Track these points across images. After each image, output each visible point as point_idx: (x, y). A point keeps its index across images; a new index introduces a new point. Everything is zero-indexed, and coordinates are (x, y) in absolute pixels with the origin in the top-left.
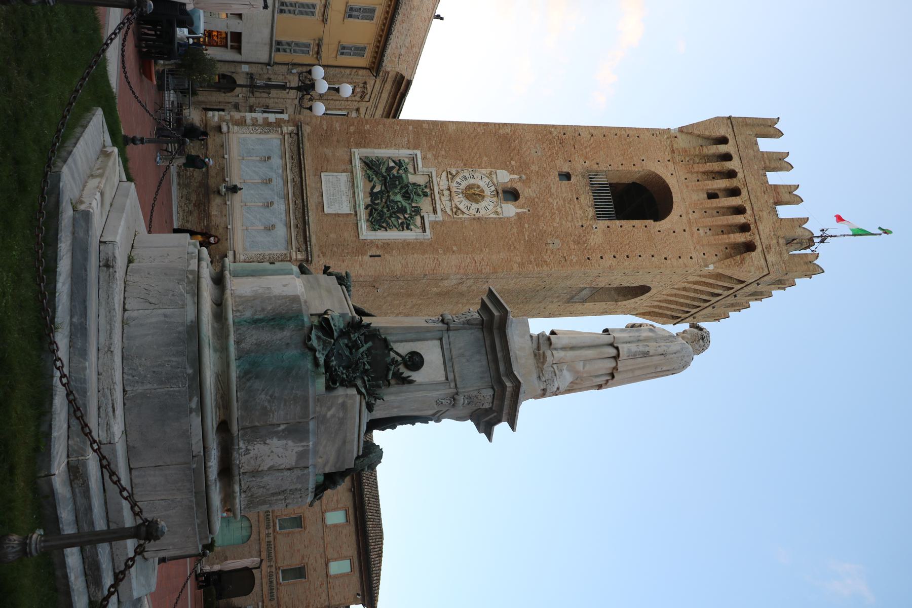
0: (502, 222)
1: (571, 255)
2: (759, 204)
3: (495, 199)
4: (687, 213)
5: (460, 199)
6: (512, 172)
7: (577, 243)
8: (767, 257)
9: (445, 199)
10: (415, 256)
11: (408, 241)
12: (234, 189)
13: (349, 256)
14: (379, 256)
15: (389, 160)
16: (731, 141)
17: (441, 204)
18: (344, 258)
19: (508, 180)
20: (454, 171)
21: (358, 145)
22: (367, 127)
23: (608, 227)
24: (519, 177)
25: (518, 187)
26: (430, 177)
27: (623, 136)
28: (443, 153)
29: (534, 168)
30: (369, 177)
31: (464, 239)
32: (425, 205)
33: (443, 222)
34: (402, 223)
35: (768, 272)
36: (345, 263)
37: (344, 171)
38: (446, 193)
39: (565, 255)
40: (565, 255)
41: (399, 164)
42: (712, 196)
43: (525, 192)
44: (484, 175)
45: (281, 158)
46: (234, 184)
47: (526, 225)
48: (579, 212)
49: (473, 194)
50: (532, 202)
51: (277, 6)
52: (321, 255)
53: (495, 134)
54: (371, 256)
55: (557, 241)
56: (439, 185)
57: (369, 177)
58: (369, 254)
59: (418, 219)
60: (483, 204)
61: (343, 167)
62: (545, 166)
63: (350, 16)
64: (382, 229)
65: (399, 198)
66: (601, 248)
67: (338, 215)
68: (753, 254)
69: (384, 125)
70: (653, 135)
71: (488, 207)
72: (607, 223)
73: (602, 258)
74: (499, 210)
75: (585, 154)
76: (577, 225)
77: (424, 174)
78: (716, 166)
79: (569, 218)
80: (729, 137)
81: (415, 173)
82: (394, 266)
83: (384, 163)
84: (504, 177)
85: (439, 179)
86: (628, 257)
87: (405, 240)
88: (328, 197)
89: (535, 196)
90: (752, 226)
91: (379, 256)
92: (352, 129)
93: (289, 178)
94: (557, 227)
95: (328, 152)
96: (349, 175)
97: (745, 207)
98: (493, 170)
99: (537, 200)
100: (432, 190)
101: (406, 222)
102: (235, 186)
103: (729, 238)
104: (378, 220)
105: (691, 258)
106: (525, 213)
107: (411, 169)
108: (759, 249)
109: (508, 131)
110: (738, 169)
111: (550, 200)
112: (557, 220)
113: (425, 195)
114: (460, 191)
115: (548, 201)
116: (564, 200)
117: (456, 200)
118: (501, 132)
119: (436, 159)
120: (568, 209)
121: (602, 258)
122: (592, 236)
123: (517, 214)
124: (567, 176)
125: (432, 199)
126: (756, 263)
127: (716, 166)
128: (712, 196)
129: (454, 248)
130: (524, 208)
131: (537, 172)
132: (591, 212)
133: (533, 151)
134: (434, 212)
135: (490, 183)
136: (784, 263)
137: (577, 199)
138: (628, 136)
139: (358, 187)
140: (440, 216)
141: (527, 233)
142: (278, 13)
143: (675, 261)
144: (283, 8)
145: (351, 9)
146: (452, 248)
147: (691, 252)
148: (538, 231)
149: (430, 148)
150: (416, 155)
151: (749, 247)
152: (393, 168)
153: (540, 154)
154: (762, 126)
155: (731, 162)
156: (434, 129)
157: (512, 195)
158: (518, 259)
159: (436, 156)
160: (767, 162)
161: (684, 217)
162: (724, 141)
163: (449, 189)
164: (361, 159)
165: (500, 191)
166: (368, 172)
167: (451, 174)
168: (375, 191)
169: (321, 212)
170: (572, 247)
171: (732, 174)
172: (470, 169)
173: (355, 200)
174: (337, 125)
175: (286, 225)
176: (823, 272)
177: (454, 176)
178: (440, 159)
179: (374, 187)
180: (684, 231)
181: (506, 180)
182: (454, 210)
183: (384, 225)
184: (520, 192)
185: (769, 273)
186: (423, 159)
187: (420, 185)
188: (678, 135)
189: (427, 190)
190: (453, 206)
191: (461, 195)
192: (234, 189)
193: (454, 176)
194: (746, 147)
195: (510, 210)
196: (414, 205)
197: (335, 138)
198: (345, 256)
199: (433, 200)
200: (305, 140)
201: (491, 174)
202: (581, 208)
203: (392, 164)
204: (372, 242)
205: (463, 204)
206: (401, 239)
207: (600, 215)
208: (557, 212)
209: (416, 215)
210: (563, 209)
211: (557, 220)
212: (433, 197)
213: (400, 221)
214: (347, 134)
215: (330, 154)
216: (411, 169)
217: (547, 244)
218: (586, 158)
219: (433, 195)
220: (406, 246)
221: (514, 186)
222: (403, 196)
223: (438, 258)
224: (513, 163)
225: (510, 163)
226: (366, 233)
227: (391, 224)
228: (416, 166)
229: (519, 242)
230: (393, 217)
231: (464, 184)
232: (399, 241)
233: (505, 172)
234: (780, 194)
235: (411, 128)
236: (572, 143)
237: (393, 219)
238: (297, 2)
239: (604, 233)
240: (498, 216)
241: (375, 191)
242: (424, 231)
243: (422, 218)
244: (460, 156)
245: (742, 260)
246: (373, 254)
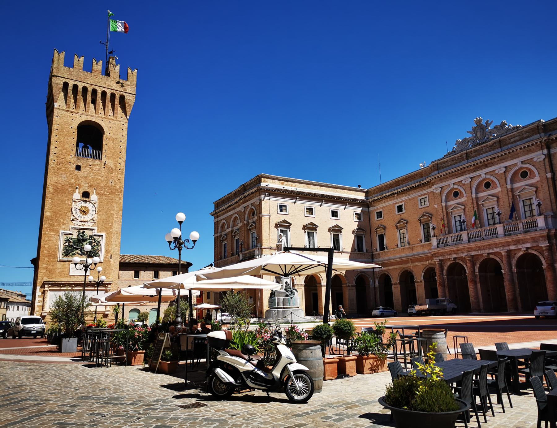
0: (100, 201)
1: (117, 177)
2: (102, 83)
4: (102, 117)
5: (87, 217)
6: (75, 192)
7: (112, 172)
8: (128, 92)
9: (86, 224)
10: (112, 241)
14: (111, 255)
16: (67, 81)
21: (55, 256)
23: (105, 156)
25: (82, 191)
26: (75, 229)
27: (57, 132)
28: (62, 220)
29: (73, 181)
30: (73, 255)
31: (106, 220)
33: (98, 227)
34: (97, 244)
36: (113, 269)
37: (70, 265)
38: (83, 223)
40: (117, 179)
41: (68, 241)
43: (85, 188)
47: (102, 192)
48: (97, 167)
49: (84, 212)
50: (90, 186)
52: (109, 278)
53: (53, 194)
54: (111, 258)
55: (111, 181)
57: (73, 255)
58: (110, 259)
59: (95, 237)
60: (90, 208)
61: (67, 265)
64: (99, 252)
66: (115, 163)
69: (45, 244)
70: (57, 117)
72: (103, 156)
73: (120, 164)
74: (94, 202)
75: (66, 154)
76: (103, 170)
78: (80, 95)
79: (100, 172)
80: (64, 81)
81: (72, 235)
83: (66, 247)
84: (77, 195)
85: (76, 225)
86: (120, 152)
89: (87, 184)
91: (111, 255)
92: (46, 259)
94: (104, 179)
95: (58, 271)
98: (73, 200)
99: (90, 184)
100: (82, 229)
103: (117, 104)
105: (123, 124)
106: (96, 191)
107: (70, 236)
108: (125, 94)
110: (84, 84)
111: (90, 178)
112: (100, 178)
113: (83, 232)
114: (83, 217)
115: (91, 179)
116: (91, 172)
117: (87, 219)
119: (65, 224)
120: (95, 171)
121: (120, 164)
122: (109, 165)
124: (78, 168)
126: (130, 98)
127: (80, 95)
128: (94, 102)
129: (110, 224)
130: (94, 191)
131: (75, 180)
132: (97, 162)
133: (63, 178)
136: (132, 85)
137: (90, 165)
138: (57, 130)
140: (96, 228)
143: (124, 132)
147: (121, 124)
148: (105, 188)
149: (59, 225)
150: (63, 233)
151: (122, 98)
152: (68, 244)
153: (65, 176)
154: (59, 60)
155: (79, 86)
156: (49, 222)
157: (86, 195)
158: (117, 199)
159: (64, 224)
160: (80, 68)
161: (103, 120)
162: (66, 85)
163: (82, 222)
165: (84, 199)
166: (70, 255)
167: (74, 219)
168: (80, 253)
170: (114, 175)
171: (85, 89)
174: (44, 265)
178: (65, 222)
179: (78, 253)
180: (110, 122)
181: (79, 195)
182: (92, 221)
183: (97, 251)
187: (79, 234)
189: (82, 231)
190: (90, 221)
191: (85, 217)
194: (71, 74)
195: (94, 197)
196: (88, 238)
197: (51, 267)
199: (87, 229)
200: (51, 280)
201: (75, 201)
202: (96, 165)
203: (67, 244)
204: (105, 257)
205: (88, 217)
207: (100, 158)
208: (96, 177)
209: (93, 238)
210: (95, 173)
211: (100, 178)
213: (96, 245)
215: (60, 270)
216: (70, 236)
217: (111, 186)
218: (69, 155)
220: (107, 244)
222: (84, 242)
224: (70, 190)
225: (70, 191)
229: (110, 197)
231: (79, 214)
233: (75, 195)
234: (98, 70)
235: (47, 233)
236: (60, 159)
239: (108, 159)
240: (97, 203)
241: (80, 253)
242: (102, 236)
243: (95, 235)
244: (64, 213)
245: (128, 103)
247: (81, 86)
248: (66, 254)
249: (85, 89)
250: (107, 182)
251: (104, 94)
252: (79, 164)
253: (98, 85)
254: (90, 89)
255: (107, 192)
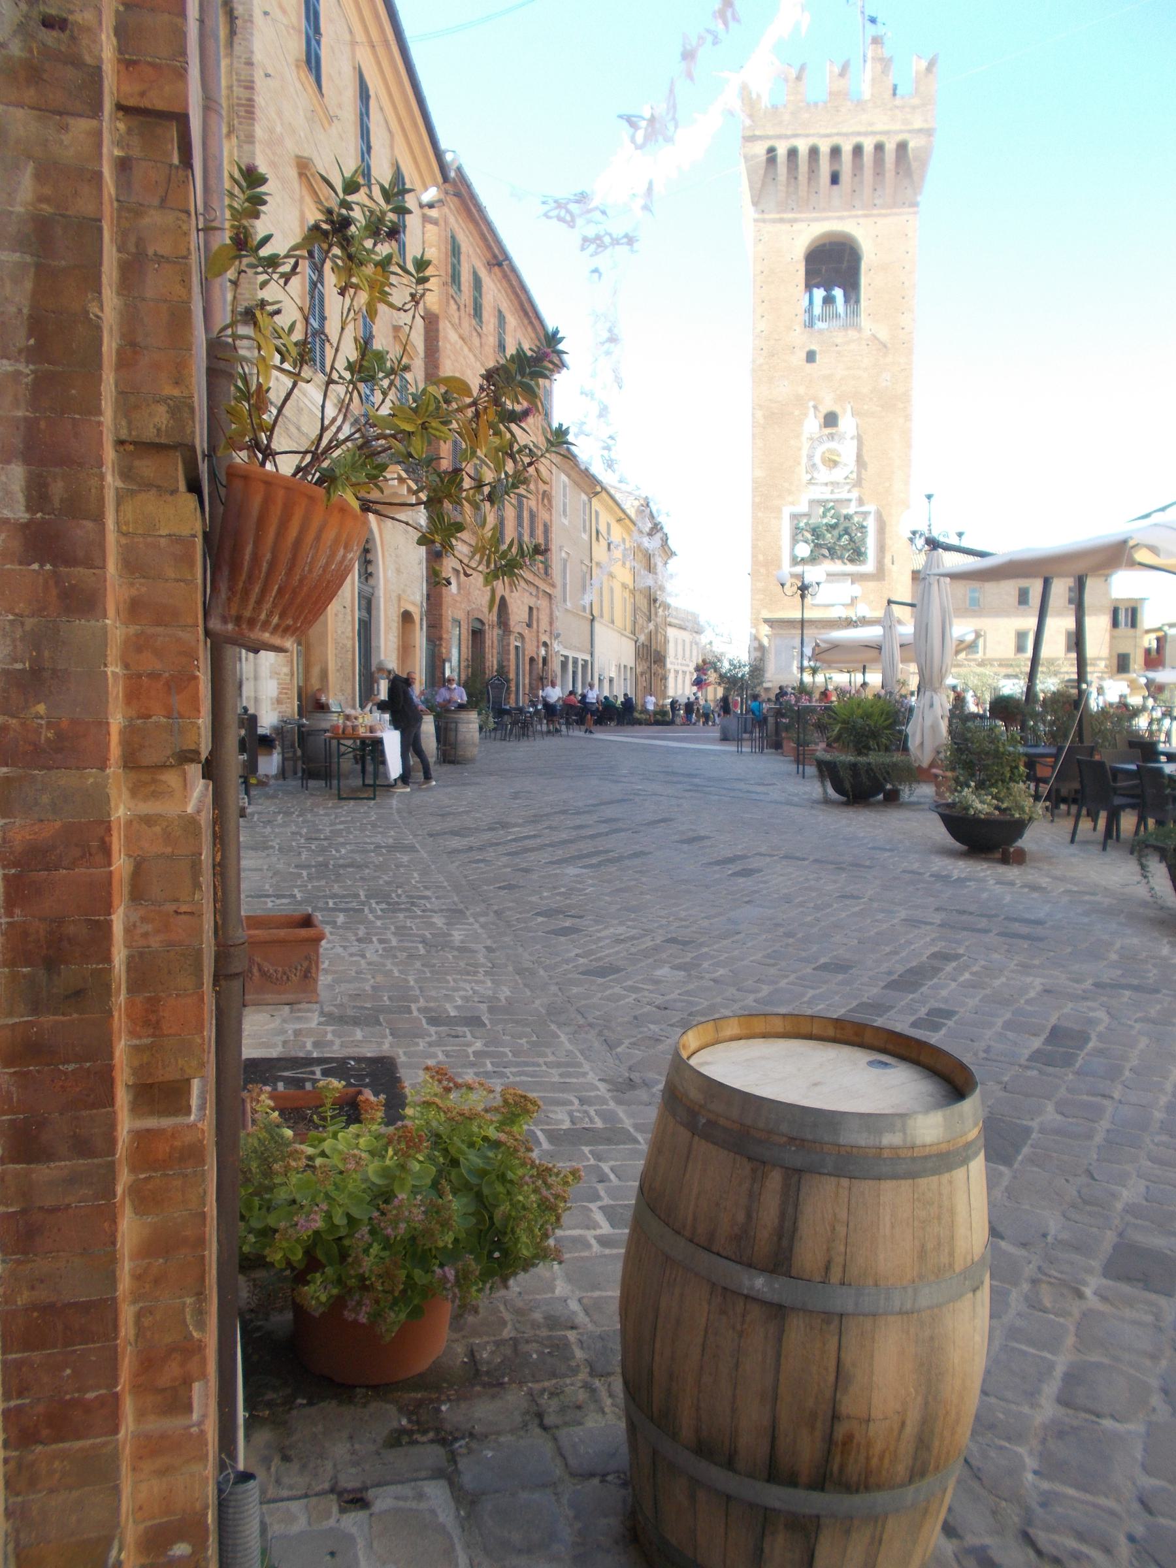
6: (806, 415)
21: (779, 567)
22: (761, 557)
25: (824, 410)
26: (812, 502)
29: (802, 390)
42: (835, 179)
68: (911, 145)
84: (812, 424)
90: (879, 138)
104: (857, 555)
109: (759, 414)
118: (762, 421)
124: (811, 357)
128: (835, 179)
132: (852, 333)
151: (902, 147)
157: (831, 420)
165: (828, 431)
171: (814, 152)
186: (793, 504)
195: (847, 424)
221: (821, 416)
247: (803, 147)
249: (814, 152)
251: (858, 150)
252: (813, 347)
253: (844, 130)
254: (825, 149)
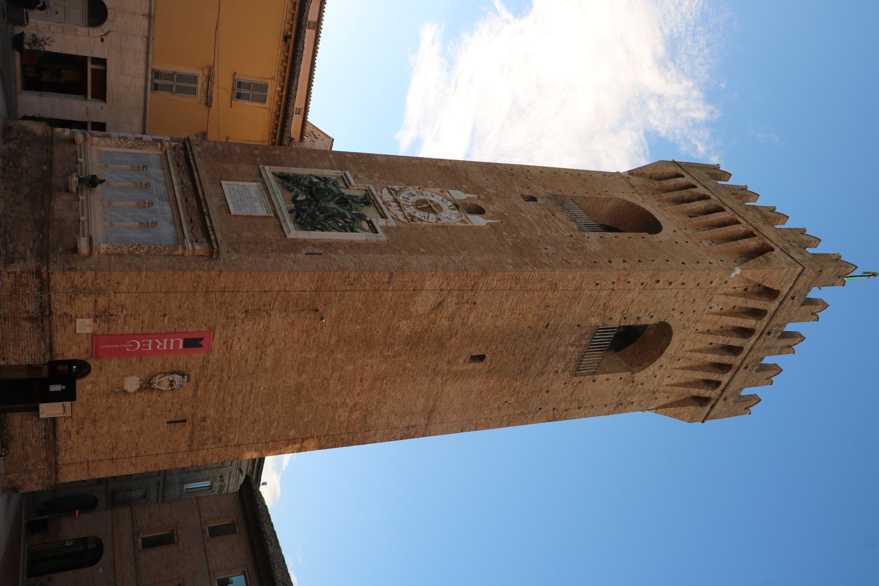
3: (456, 212)
11: (356, 242)
12: (93, 182)
13: (275, 254)
14: (321, 254)
15: (312, 177)
17: (391, 213)
18: (268, 255)
19: (466, 198)
20: (396, 187)
24: (476, 196)
32: (370, 213)
33: (398, 229)
35: (802, 268)
39: (565, 258)
43: (490, 208)
44: (435, 193)
45: (163, 169)
46: (91, 174)
50: (500, 216)
51: (150, 77)
56: (381, 197)
62: (502, 190)
63: (239, 96)
65: (332, 205)
67: (252, 217)
71: (450, 216)
77: (360, 188)
82: (344, 263)
85: (380, 194)
87: (351, 241)
88: (234, 202)
91: (321, 254)
93: (175, 181)
96: (260, 185)
97: (736, 219)
101: (349, 225)
102: (94, 177)
106: (498, 224)
123: (488, 224)
125: (377, 209)
129: (422, 250)
134: (383, 217)
135: (444, 199)
137: (553, 215)
139: (274, 193)
141: (509, 239)
142: (151, 90)
144: (157, 81)
145: (240, 84)
146: (419, 250)
164: (273, 173)
169: (226, 213)
172: (417, 187)
173: (273, 205)
175: (173, 222)
176: (856, 267)
177: (398, 192)
182: (409, 218)
183: (319, 227)
184: (483, 207)
185: (804, 268)
188: (630, 176)
192: (93, 182)
193: (398, 192)
195: (478, 221)
196: (353, 212)
198: (269, 253)
206: (346, 240)
212: (377, 206)
213: (340, 225)
214: (251, 155)
219: (376, 204)
222: (338, 203)
223: (403, 258)
226: (294, 233)
227: (328, 226)
228: (347, 181)
230: (330, 220)
231: (412, 199)
232: (344, 241)
237: (330, 222)
238: (175, 72)
246: (309, 252)
248: (283, 178)
250: (539, 241)
255: (512, 242)
